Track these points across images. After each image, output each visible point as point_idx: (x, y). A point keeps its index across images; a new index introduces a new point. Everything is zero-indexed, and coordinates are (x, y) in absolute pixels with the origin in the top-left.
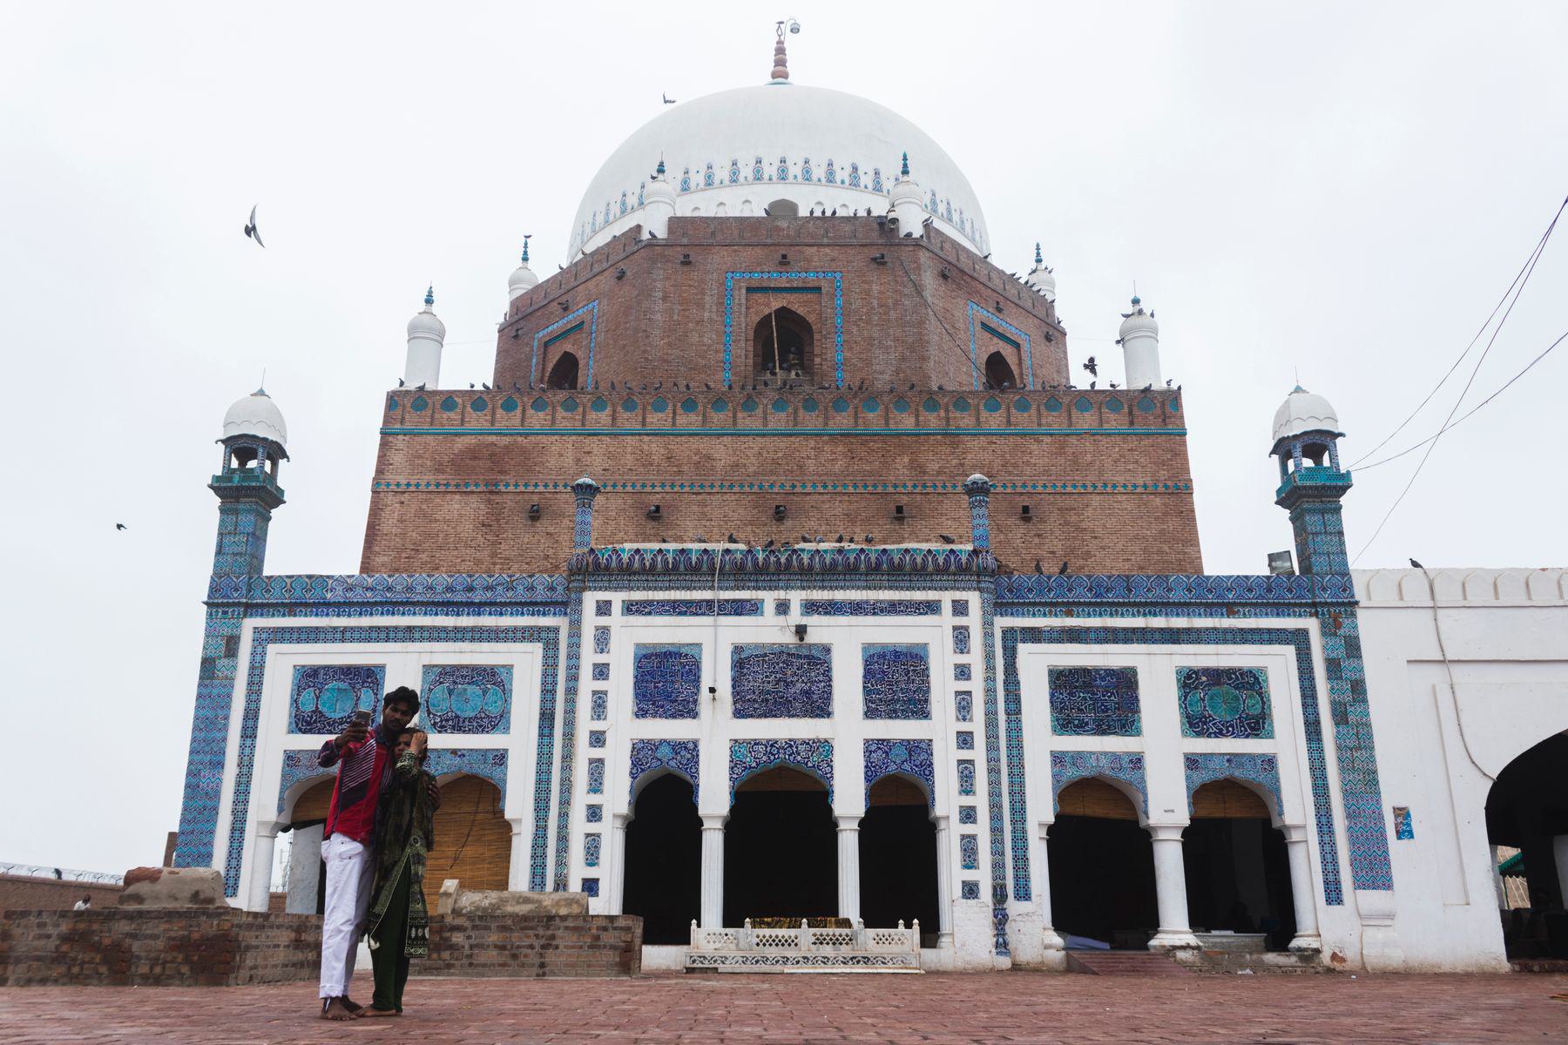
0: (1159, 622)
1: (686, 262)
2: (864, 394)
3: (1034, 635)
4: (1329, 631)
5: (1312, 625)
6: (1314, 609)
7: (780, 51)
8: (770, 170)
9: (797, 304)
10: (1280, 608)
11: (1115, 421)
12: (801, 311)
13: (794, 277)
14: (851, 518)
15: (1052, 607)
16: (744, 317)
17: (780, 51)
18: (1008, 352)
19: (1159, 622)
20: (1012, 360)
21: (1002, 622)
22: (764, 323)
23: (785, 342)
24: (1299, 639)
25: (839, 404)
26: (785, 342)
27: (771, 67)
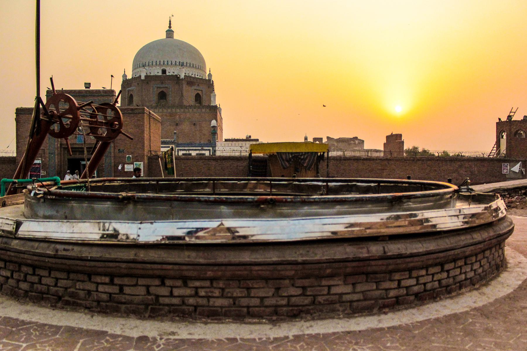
0: (194, 148)
1: (148, 83)
2: (173, 106)
3: (181, 150)
4: (213, 149)
5: (211, 148)
6: (211, 147)
7: (170, 22)
8: (162, 63)
9: (164, 90)
10: (208, 147)
11: (208, 110)
12: (165, 91)
13: (164, 85)
14: (170, 125)
15: (183, 147)
16: (157, 91)
17: (170, 22)
18: (200, 92)
19: (194, 148)
20: (201, 94)
21: (177, 148)
22: (159, 93)
23: (162, 96)
24: (209, 150)
25: (169, 107)
26: (162, 96)
27: (168, 25)
